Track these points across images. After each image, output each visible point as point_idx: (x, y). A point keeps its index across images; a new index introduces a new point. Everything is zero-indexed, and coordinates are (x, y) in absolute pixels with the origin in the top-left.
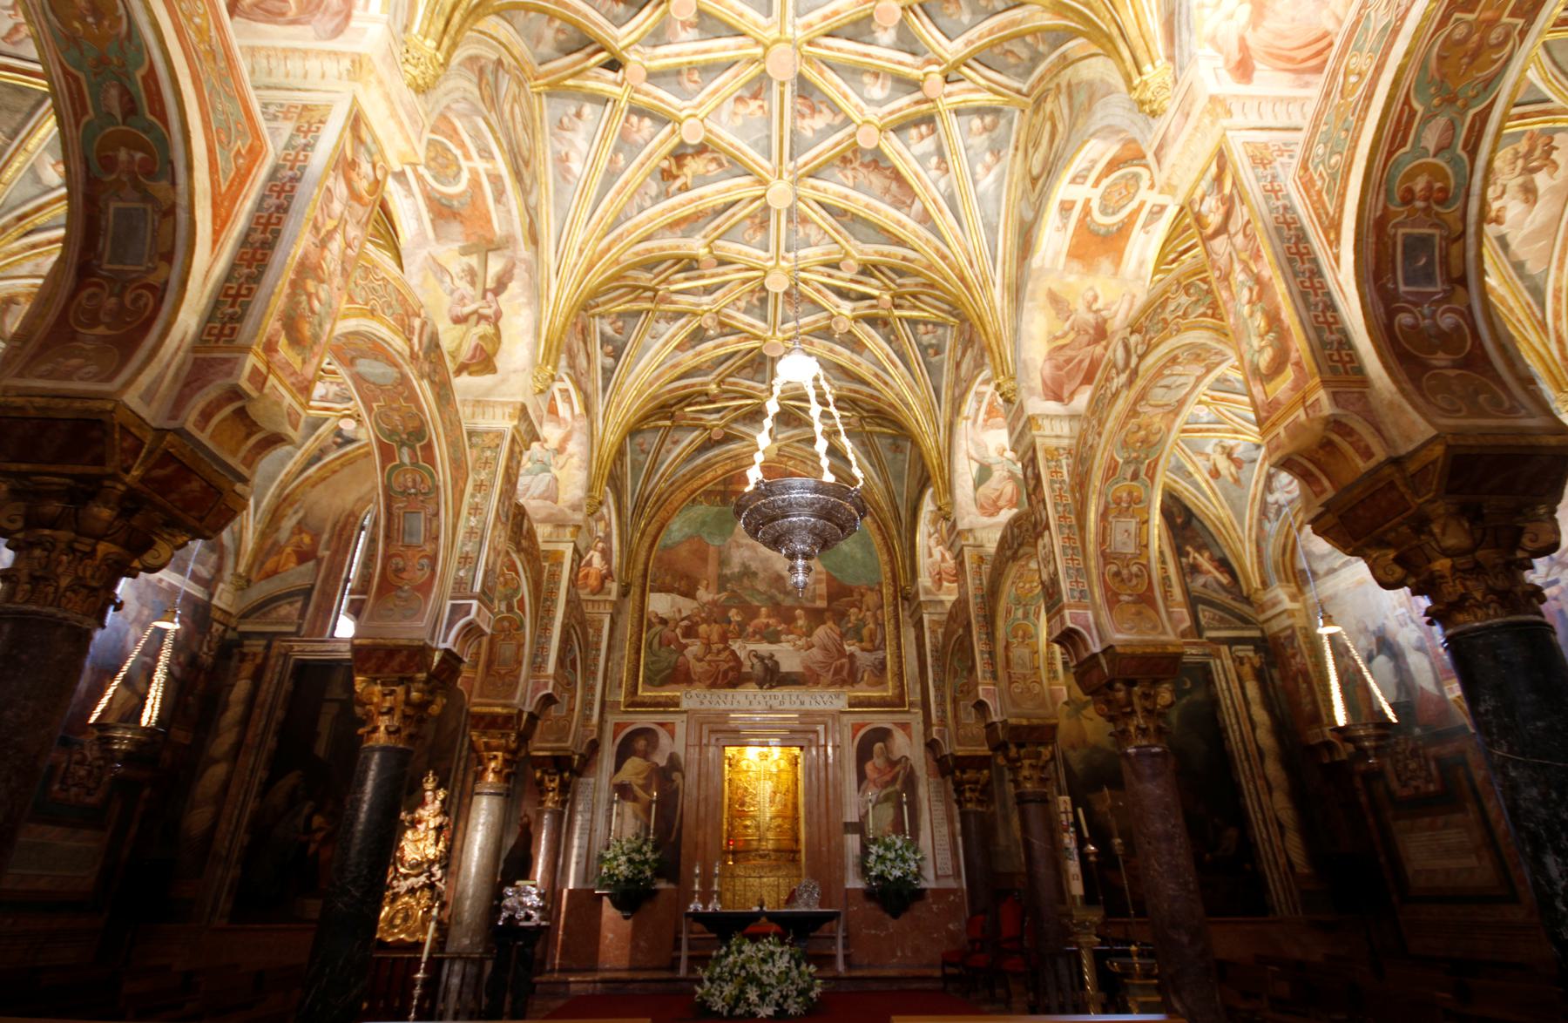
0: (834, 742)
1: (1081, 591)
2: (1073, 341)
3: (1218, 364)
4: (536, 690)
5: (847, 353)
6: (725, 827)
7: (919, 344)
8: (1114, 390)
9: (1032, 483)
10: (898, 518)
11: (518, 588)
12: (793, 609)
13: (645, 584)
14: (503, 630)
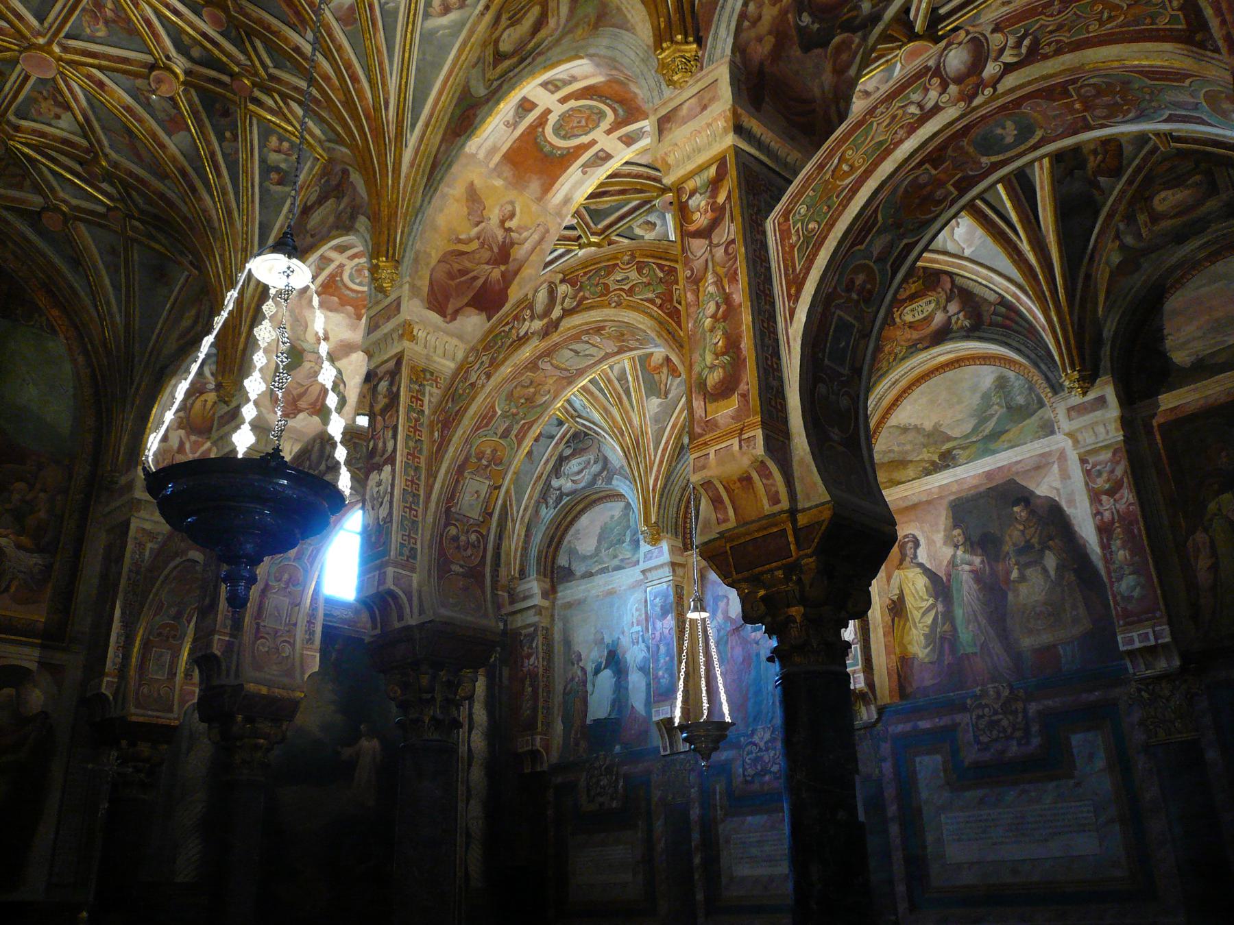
1: (412, 549)
2: (473, 252)
3: (631, 349)
7: (263, 161)
8: (522, 333)
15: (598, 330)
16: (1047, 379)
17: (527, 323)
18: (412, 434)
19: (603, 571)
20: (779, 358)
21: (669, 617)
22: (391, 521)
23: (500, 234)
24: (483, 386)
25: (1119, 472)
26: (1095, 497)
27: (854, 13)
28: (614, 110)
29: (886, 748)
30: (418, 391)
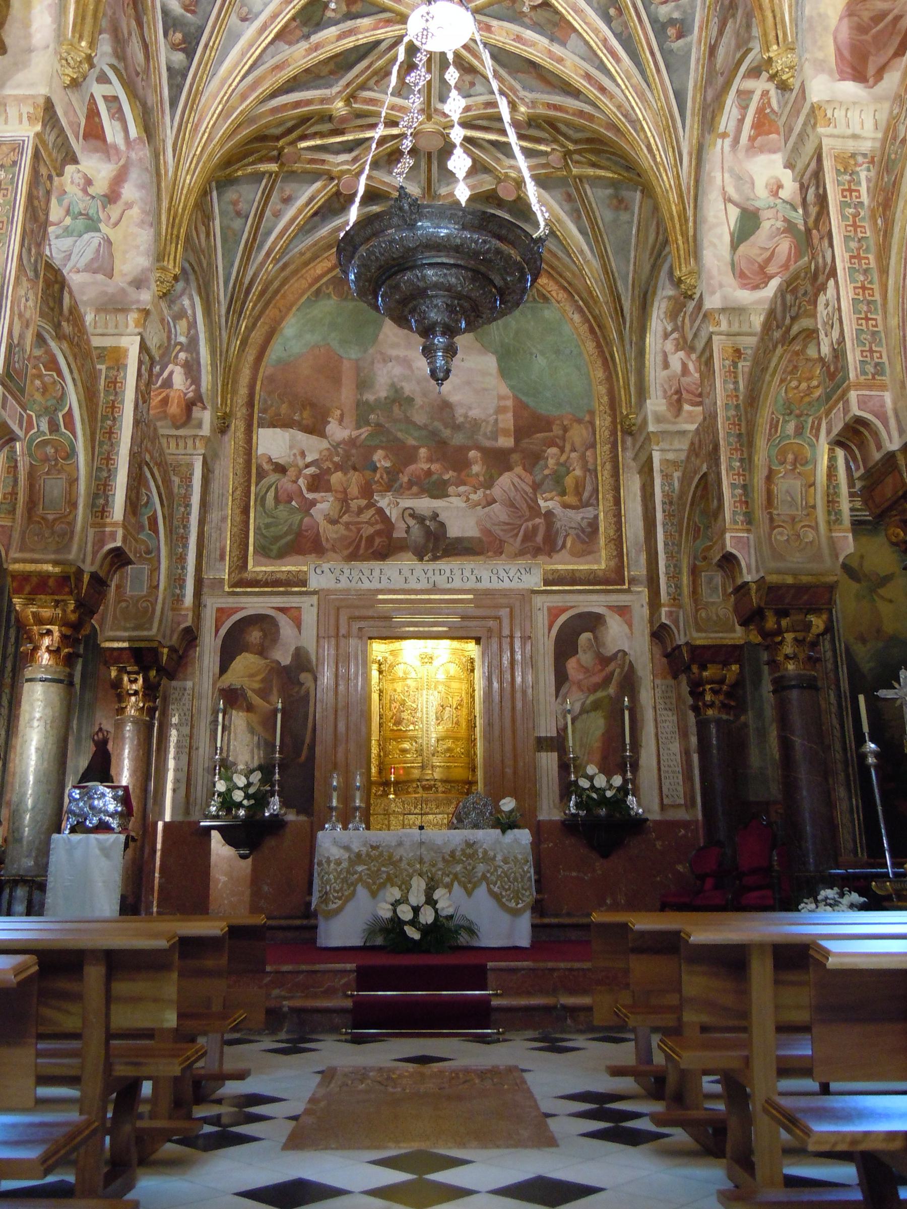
0: (523, 630)
1: (877, 364)
4: (100, 541)
5: (543, 41)
6: (375, 751)
7: (654, 21)
9: (813, 210)
10: (619, 311)
11: (64, 394)
12: (463, 450)
13: (251, 416)
14: (46, 459)
22: (844, 338)
30: (849, 182)
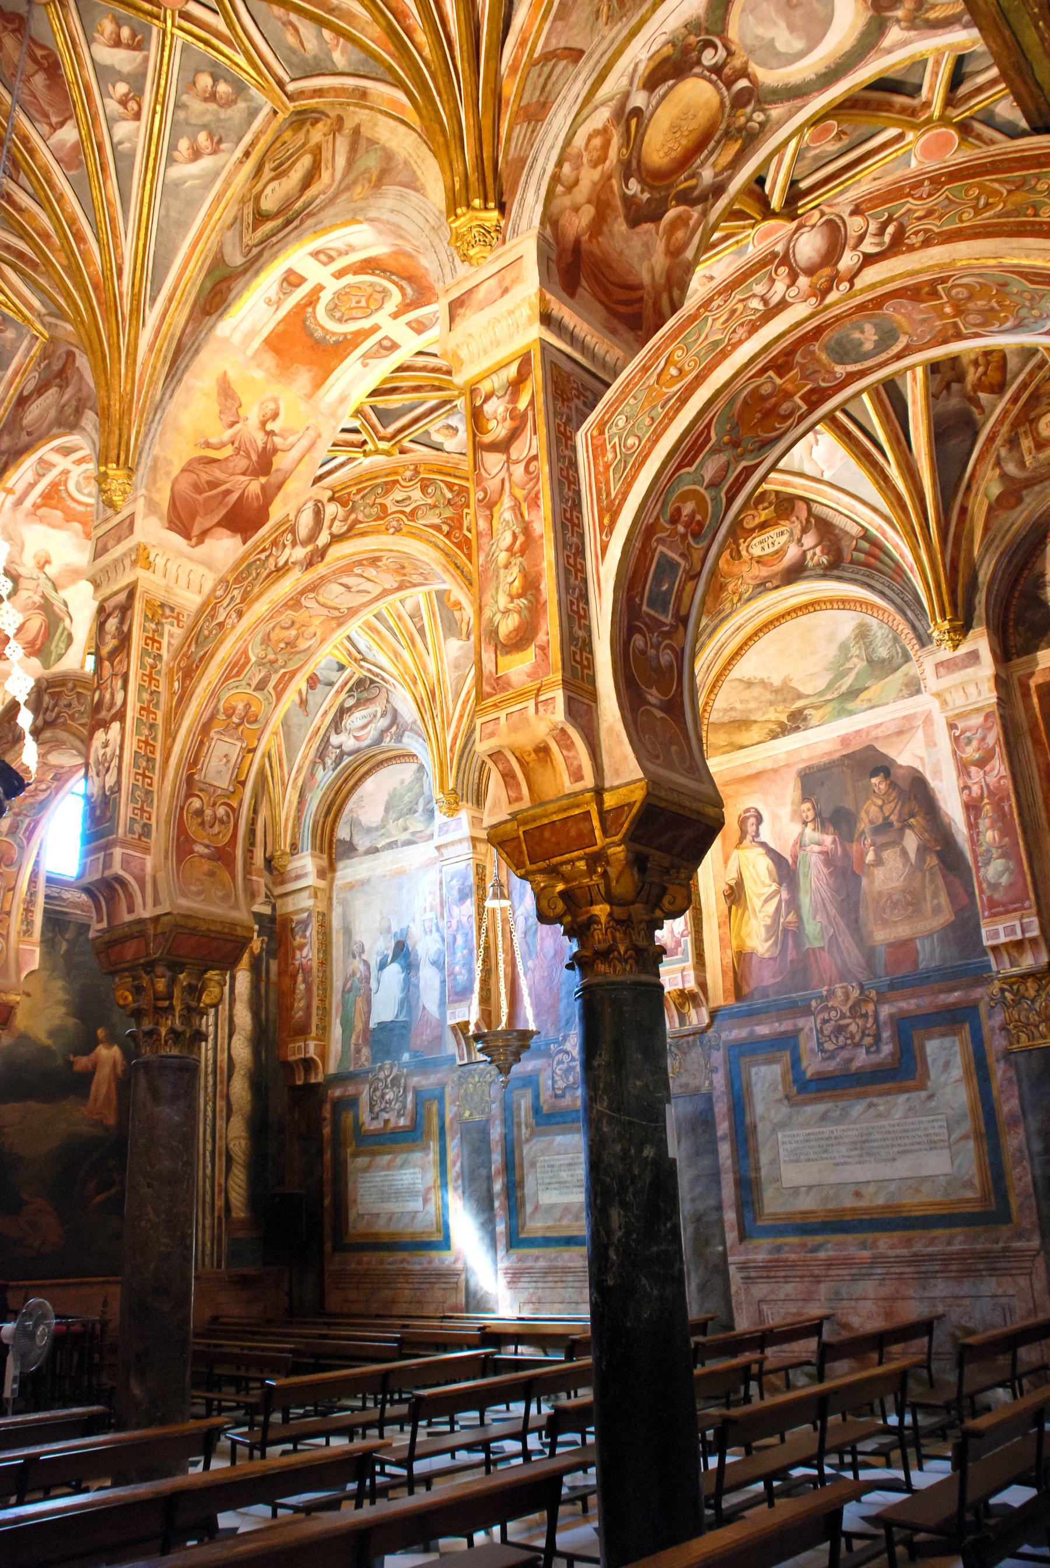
1: (145, 825)
8: (281, 563)
15: (374, 561)
16: (914, 628)
17: (287, 551)
18: (146, 684)
19: (392, 845)
20: (587, 603)
21: (468, 902)
22: (120, 789)
23: (260, 438)
24: (233, 627)
25: (991, 740)
26: (963, 768)
27: (692, 182)
28: (402, 289)
29: (718, 1057)
30: (154, 631)
